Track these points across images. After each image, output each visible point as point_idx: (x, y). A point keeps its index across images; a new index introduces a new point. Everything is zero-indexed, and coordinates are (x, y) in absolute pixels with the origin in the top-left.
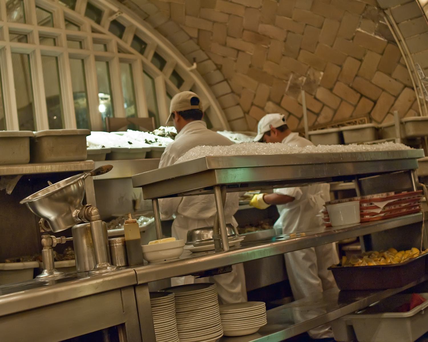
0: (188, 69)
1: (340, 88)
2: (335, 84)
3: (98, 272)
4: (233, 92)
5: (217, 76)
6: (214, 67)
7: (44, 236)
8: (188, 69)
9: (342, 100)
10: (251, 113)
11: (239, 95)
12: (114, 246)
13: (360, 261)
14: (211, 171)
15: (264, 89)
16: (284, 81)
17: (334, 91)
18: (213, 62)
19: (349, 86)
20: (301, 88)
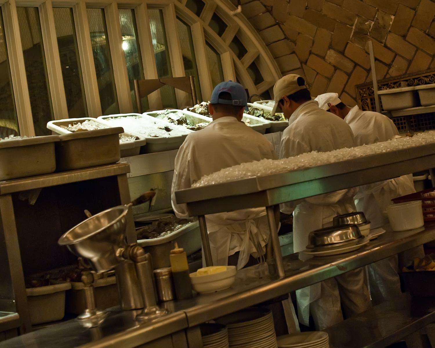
0: (232, 13)
1: (415, 34)
2: (408, 31)
3: (146, 318)
4: (286, 38)
5: (267, 20)
6: (264, 9)
7: (84, 273)
8: (232, 13)
9: (417, 49)
10: (308, 63)
11: (295, 42)
12: (160, 279)
14: (263, 192)
17: (407, 39)
18: (261, 3)
19: (425, 32)
20: (368, 34)
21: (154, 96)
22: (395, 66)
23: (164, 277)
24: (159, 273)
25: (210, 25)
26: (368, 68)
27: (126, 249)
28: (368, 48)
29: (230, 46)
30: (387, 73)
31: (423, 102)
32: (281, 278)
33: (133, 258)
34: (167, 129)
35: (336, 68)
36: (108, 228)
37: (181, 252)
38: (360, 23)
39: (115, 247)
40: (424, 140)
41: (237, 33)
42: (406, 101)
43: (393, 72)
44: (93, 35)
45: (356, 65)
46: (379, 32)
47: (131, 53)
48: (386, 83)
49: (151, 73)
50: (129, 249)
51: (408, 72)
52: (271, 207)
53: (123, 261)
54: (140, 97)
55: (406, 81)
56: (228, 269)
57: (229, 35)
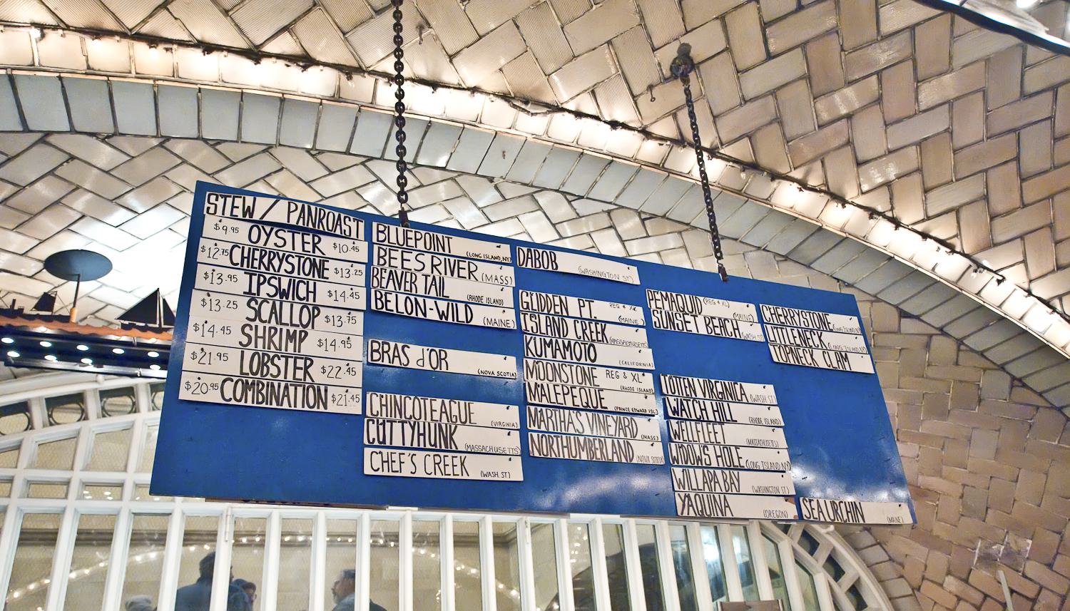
2: (1054, 558)
11: (902, 565)
15: (939, 560)
16: (969, 549)
25: (799, 543)
29: (824, 567)
38: (986, 548)
41: (831, 552)
44: (673, 544)
45: (986, 596)
46: (1013, 560)
57: (822, 554)
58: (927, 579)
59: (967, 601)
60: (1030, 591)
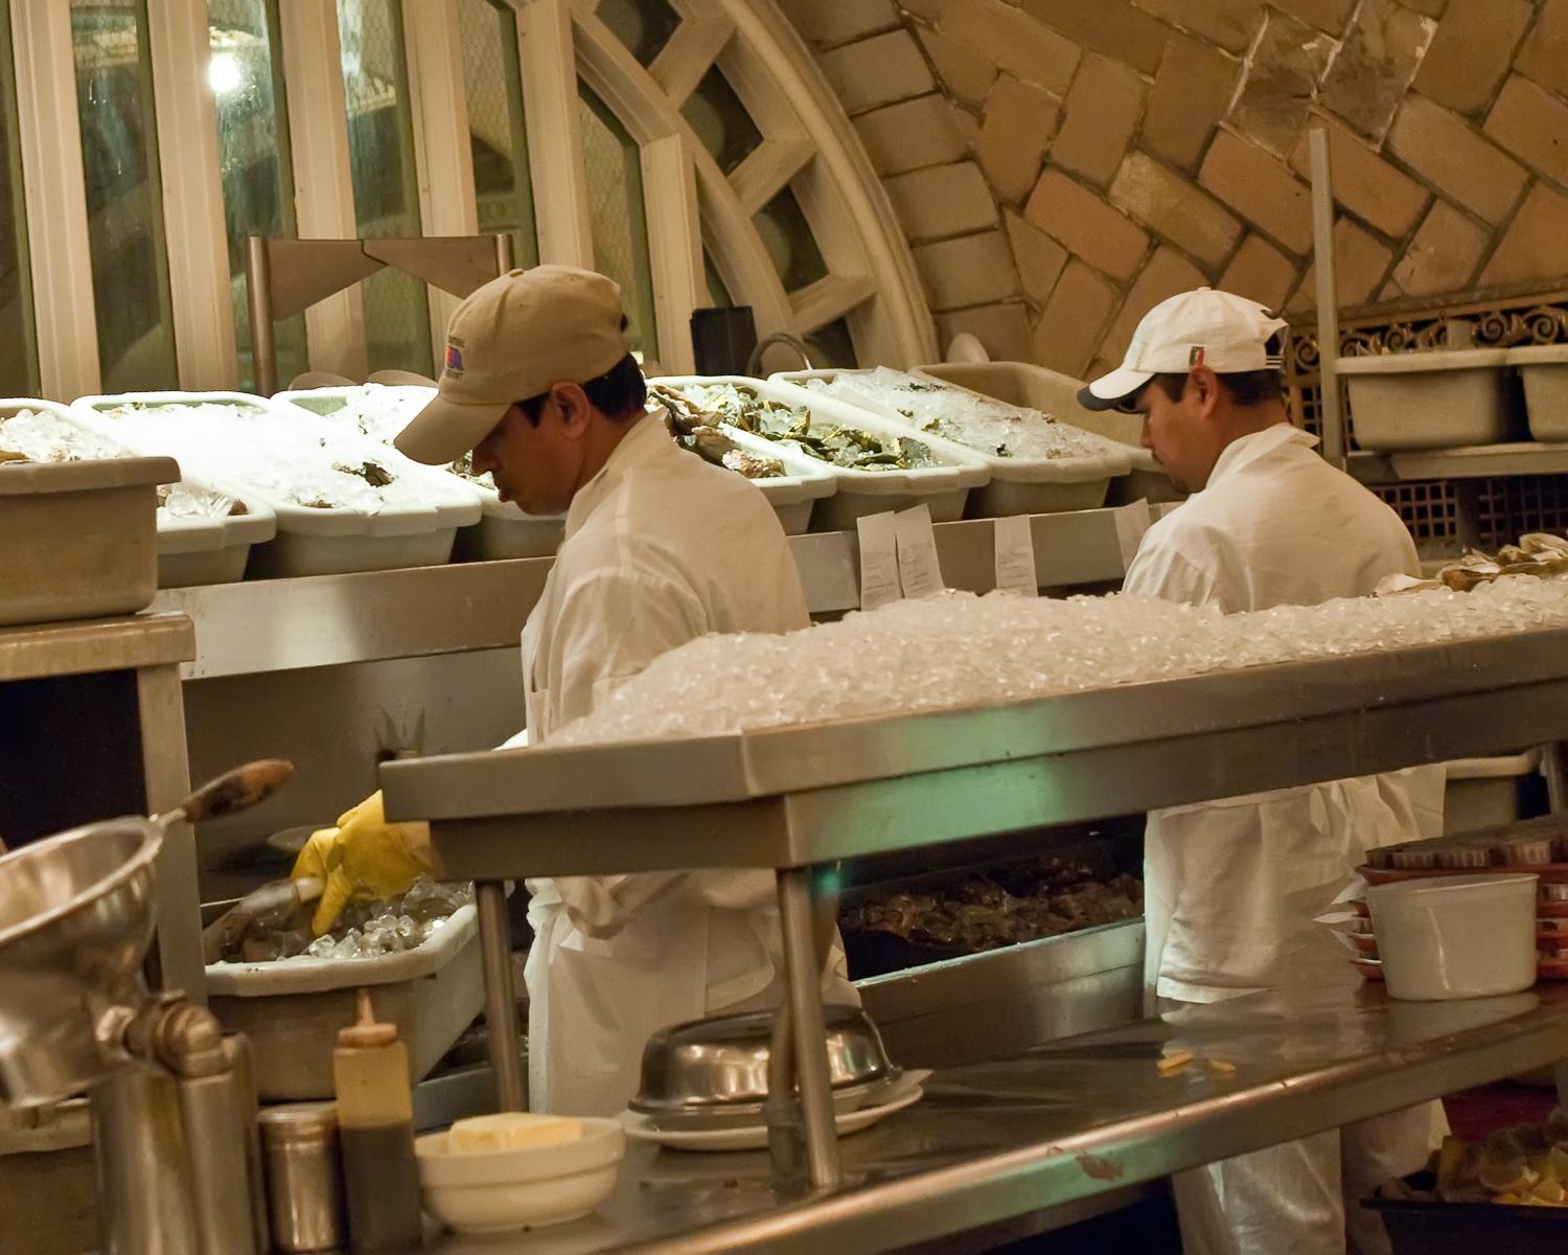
2: (1496, 92)
4: (940, 89)
11: (976, 111)
13: (1530, 1177)
15: (1114, 89)
17: (1491, 126)
20: (1314, 94)
21: (332, 317)
22: (1426, 245)
23: (302, 1146)
24: (279, 1126)
26: (1300, 250)
27: (141, 1015)
28: (1307, 160)
29: (686, 111)
30: (1388, 276)
31: (1537, 424)
32: (822, 1192)
33: (170, 1059)
34: (375, 476)
35: (1155, 241)
36: (74, 915)
37: (384, 1043)
38: (1283, 47)
39: (96, 1001)
40: (1521, 610)
41: (721, 55)
42: (1464, 414)
43: (1416, 276)
45: (1248, 229)
46: (1363, 91)
47: (244, 114)
48: (1380, 322)
49: (324, 209)
50: (154, 1014)
51: (1483, 281)
52: (798, 871)
53: (124, 1064)
54: (272, 314)
55: (1474, 318)
56: (585, 1131)
57: (686, 61)
58: (1061, 169)
59: (1180, 250)
60: (1391, 209)
